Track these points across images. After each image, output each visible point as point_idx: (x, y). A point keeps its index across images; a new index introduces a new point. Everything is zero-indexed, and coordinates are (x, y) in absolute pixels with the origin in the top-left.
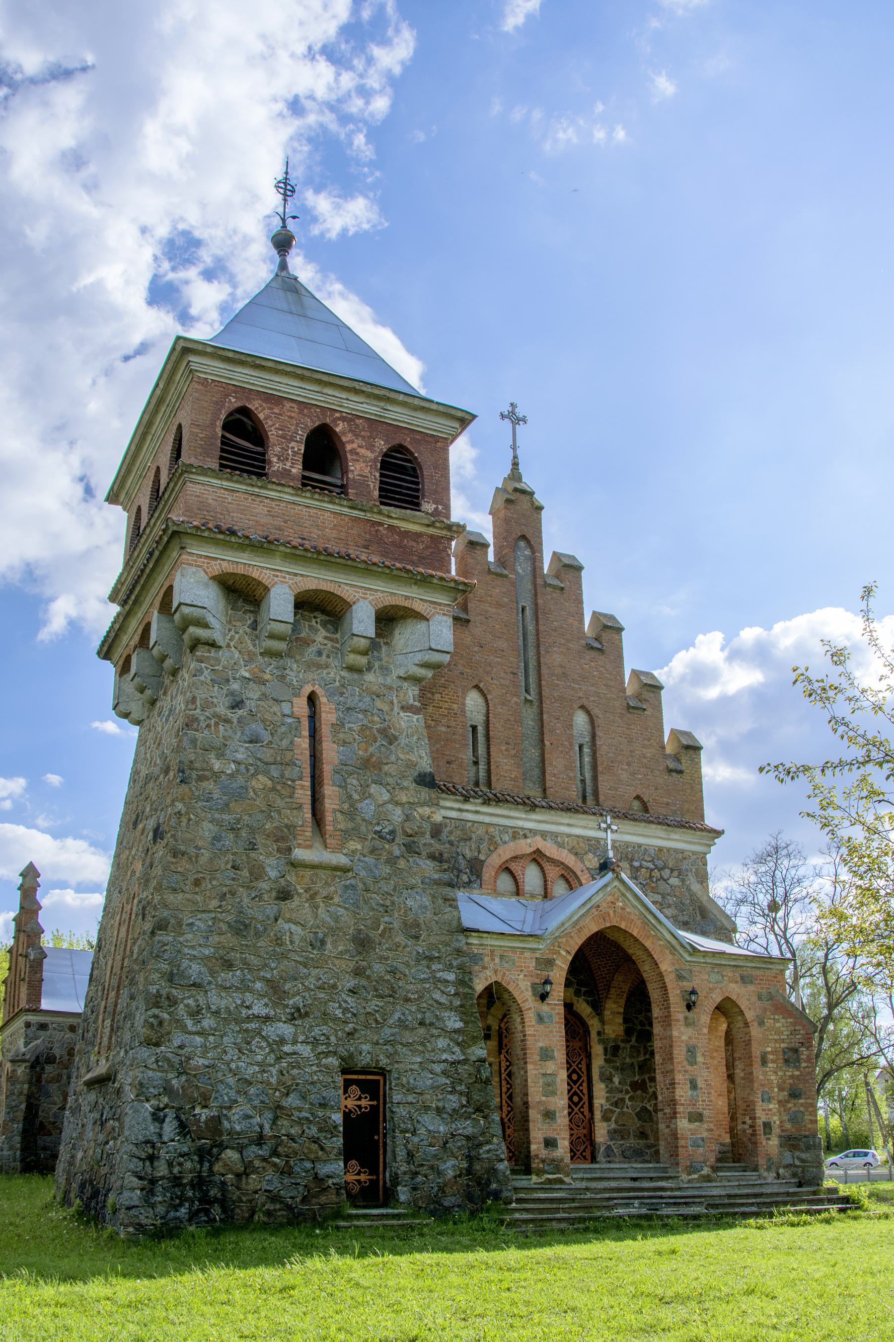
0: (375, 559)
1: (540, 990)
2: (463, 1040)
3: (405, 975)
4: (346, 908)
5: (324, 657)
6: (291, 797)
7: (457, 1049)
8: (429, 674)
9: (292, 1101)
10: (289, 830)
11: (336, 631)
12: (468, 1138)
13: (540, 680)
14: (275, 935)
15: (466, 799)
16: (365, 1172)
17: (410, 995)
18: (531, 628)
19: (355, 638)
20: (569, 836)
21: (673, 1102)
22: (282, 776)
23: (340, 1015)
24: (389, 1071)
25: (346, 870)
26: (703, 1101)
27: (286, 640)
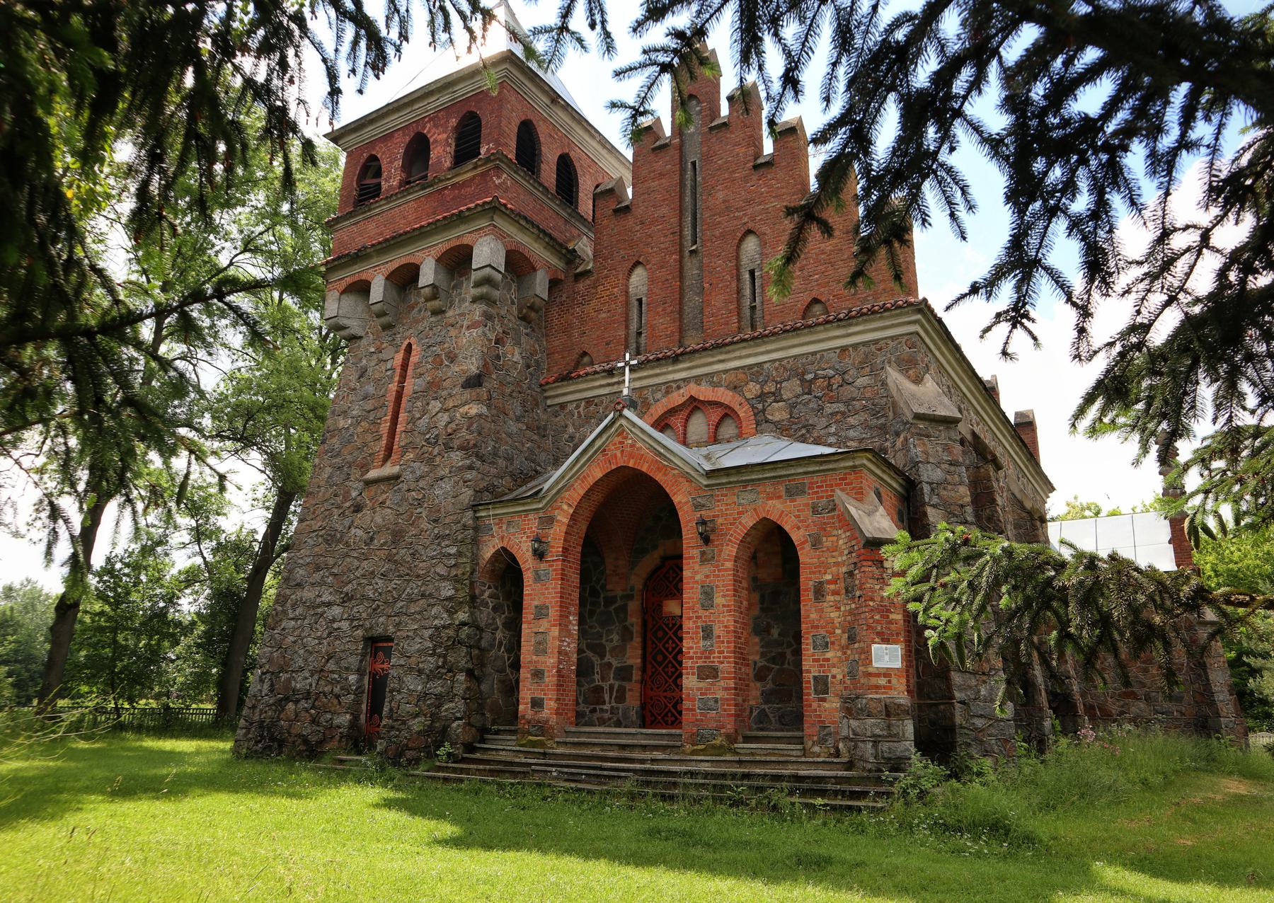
2: (452, 605)
7: (445, 615)
9: (331, 666)
12: (439, 697)
20: (725, 371)
25: (396, 478)
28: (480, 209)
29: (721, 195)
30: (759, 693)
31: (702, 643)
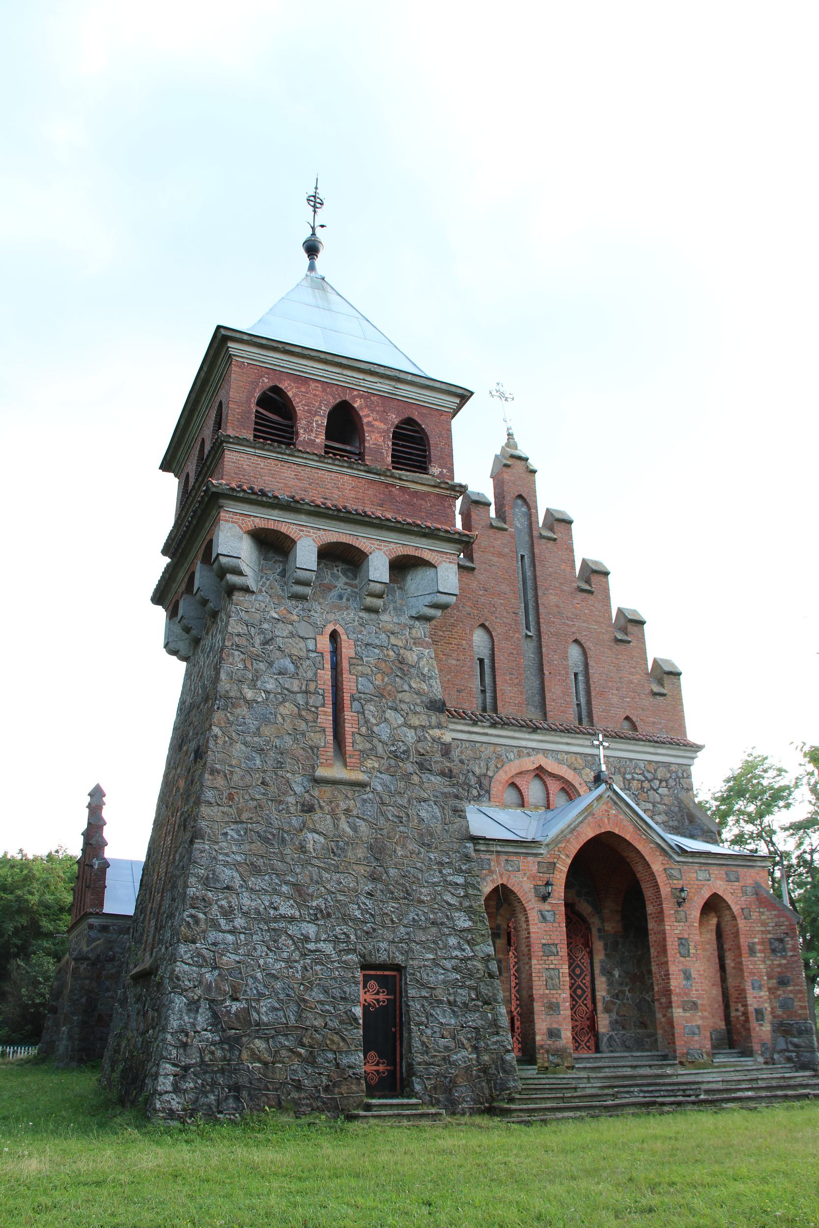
0: (389, 516)
1: (543, 890)
3: (418, 879)
4: (363, 819)
5: (344, 600)
6: (315, 722)
7: (466, 946)
8: (438, 613)
10: (313, 751)
11: (355, 577)
13: (539, 618)
14: (300, 844)
15: (475, 723)
16: (383, 1063)
17: (422, 897)
18: (529, 574)
19: (371, 583)
20: (567, 753)
21: (668, 992)
22: (307, 703)
23: (359, 916)
24: (405, 968)
25: (362, 785)
26: (697, 990)
27: (309, 585)
28: (457, 536)
29: (553, 599)
30: (607, 1022)
31: (684, 982)
